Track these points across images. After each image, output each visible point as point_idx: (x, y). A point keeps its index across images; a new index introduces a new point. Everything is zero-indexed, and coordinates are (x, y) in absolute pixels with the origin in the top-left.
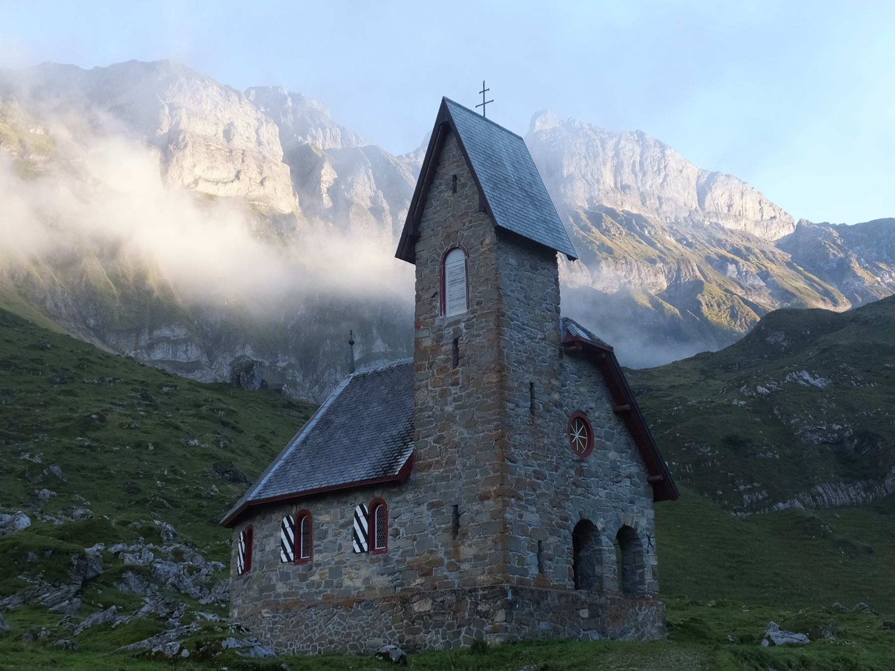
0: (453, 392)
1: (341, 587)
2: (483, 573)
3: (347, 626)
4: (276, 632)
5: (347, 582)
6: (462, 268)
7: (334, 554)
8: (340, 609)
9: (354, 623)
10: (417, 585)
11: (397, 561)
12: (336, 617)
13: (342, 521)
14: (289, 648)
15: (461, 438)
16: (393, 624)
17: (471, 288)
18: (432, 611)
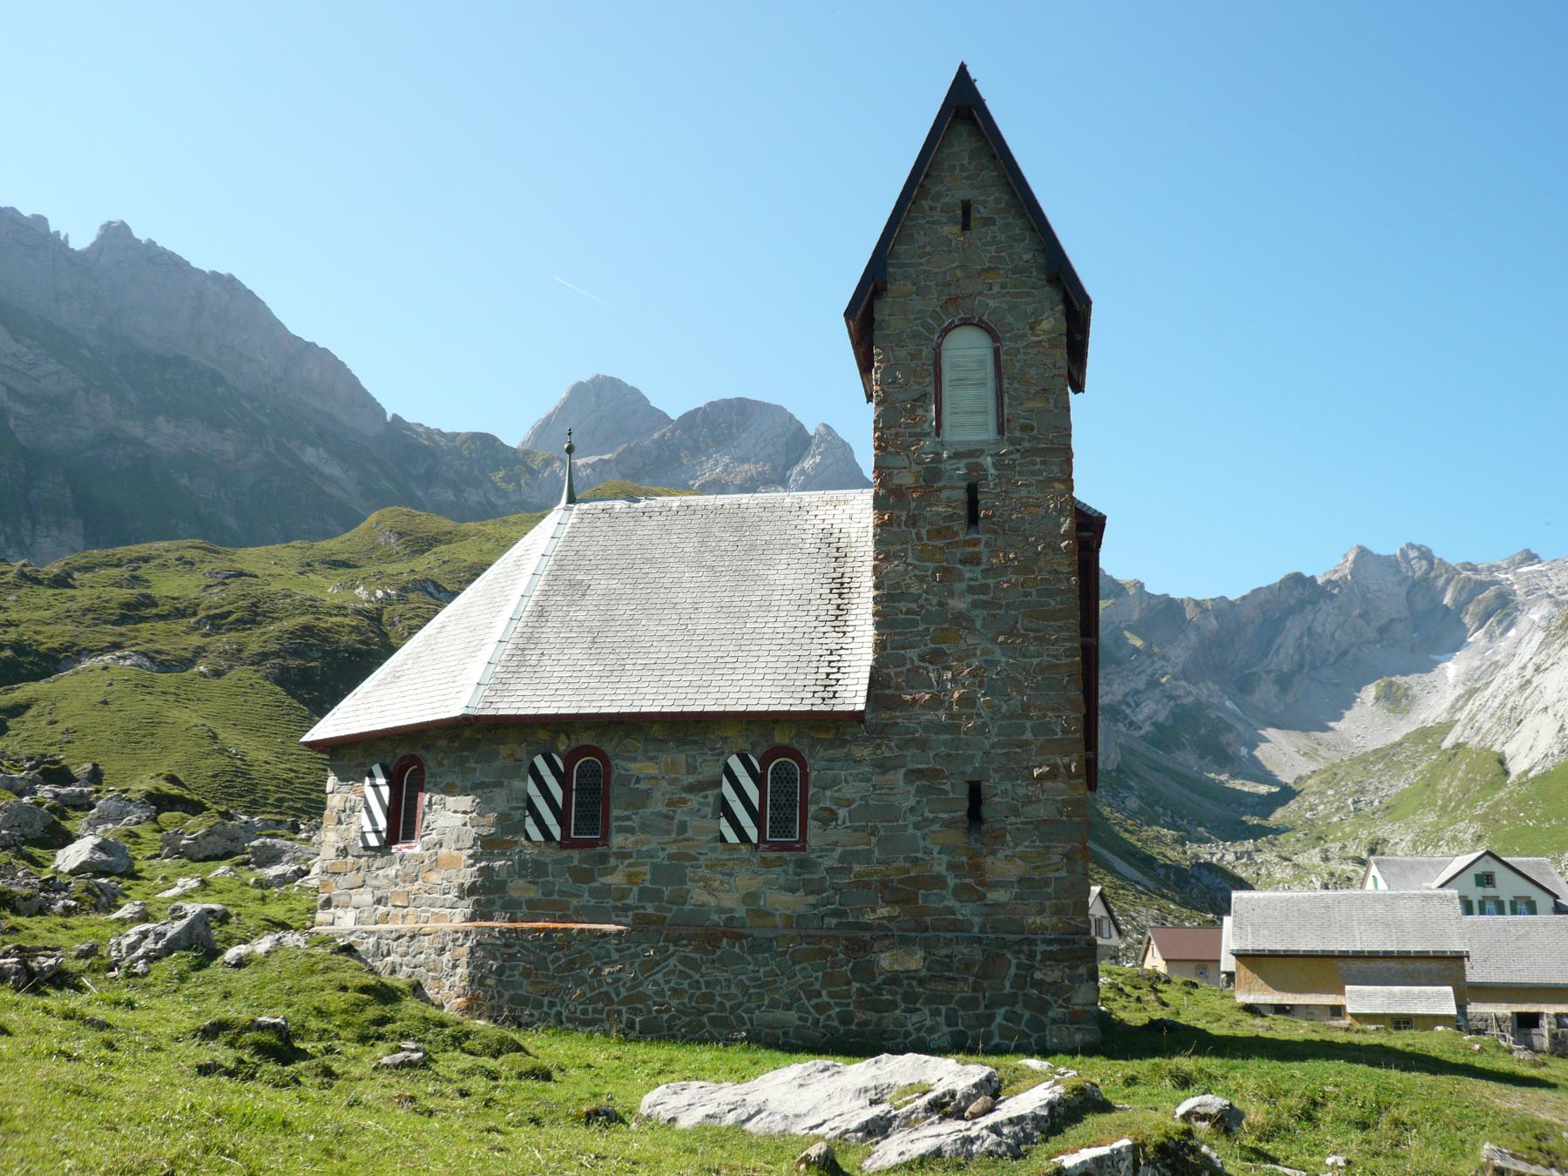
0: (967, 575)
1: (684, 903)
2: (1040, 912)
3: (701, 980)
4: (513, 976)
5: (698, 895)
6: (982, 362)
7: (666, 839)
8: (684, 946)
9: (722, 976)
10: (879, 918)
11: (830, 870)
12: (673, 961)
13: (691, 779)
14: (545, 1009)
15: (986, 661)
16: (824, 986)
17: (1006, 400)
18: (924, 973)
